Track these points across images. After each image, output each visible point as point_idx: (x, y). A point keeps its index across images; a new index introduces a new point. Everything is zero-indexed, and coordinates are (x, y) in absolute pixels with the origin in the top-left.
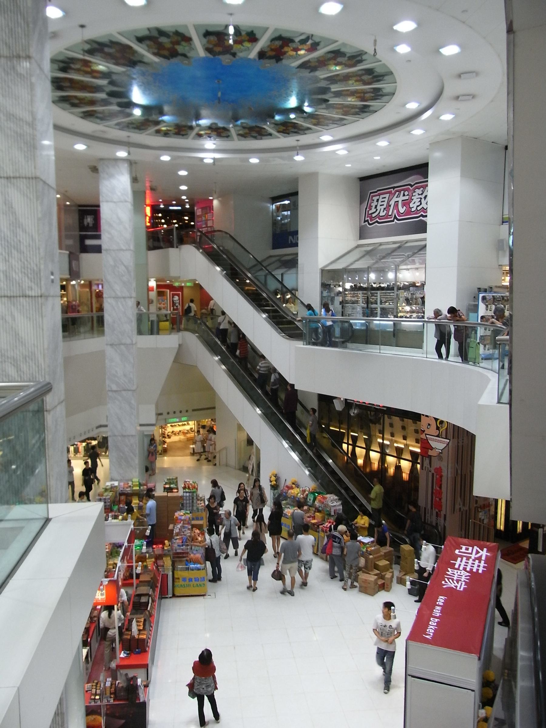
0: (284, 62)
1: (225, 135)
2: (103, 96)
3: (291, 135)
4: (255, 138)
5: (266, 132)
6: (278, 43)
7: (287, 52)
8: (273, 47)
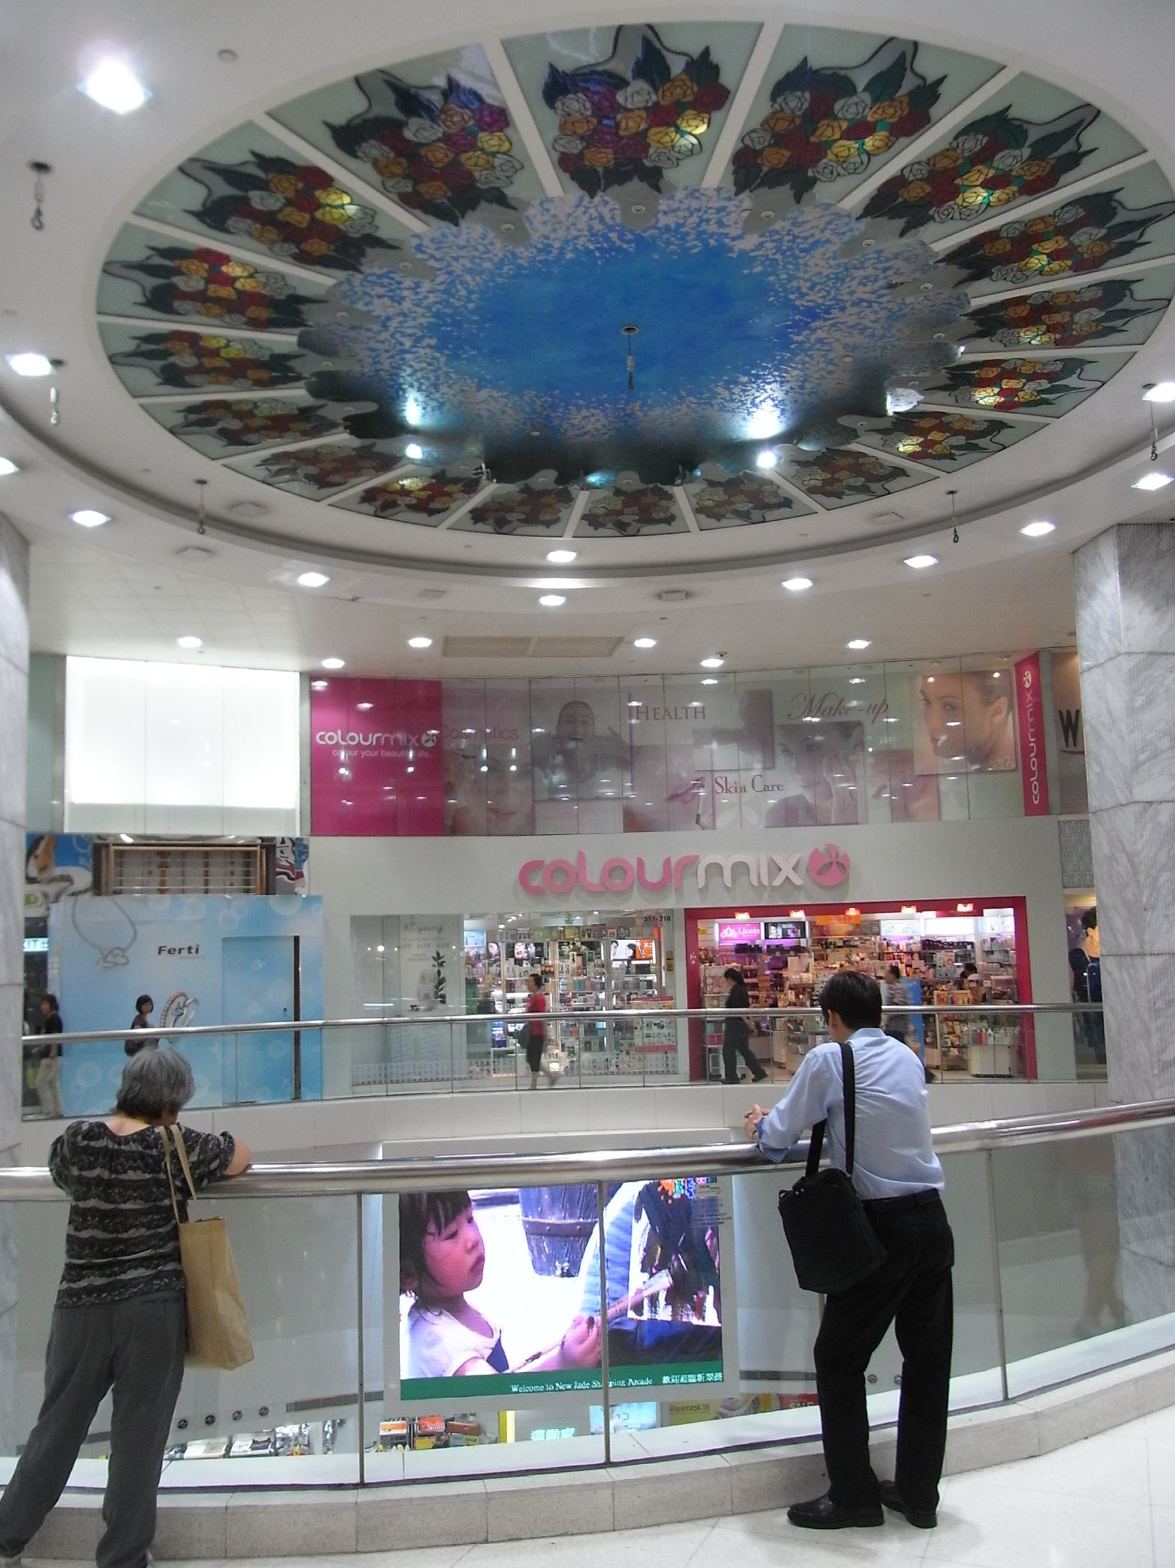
0: (823, 191)
1: (662, 515)
2: (296, 395)
3: (846, 499)
4: (746, 518)
5: (776, 495)
6: (798, 102)
7: (830, 143)
8: (782, 126)
